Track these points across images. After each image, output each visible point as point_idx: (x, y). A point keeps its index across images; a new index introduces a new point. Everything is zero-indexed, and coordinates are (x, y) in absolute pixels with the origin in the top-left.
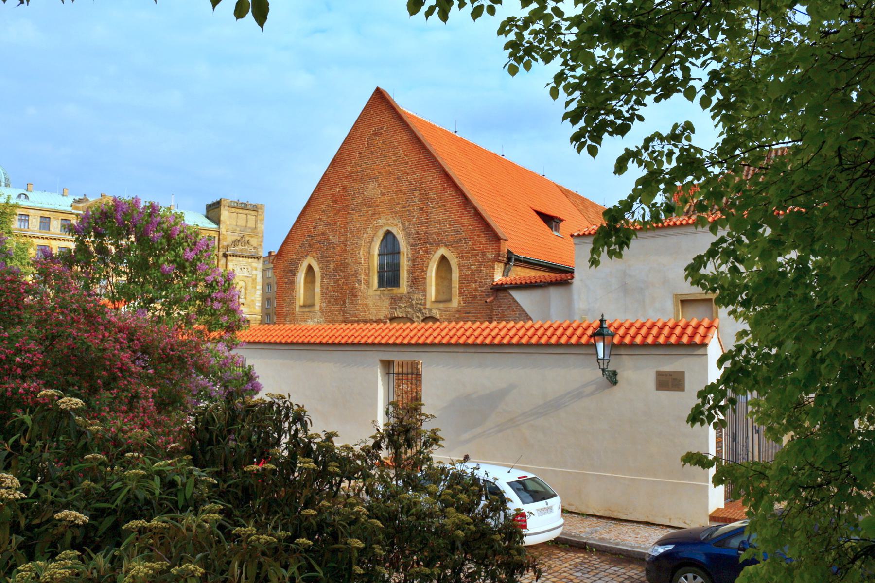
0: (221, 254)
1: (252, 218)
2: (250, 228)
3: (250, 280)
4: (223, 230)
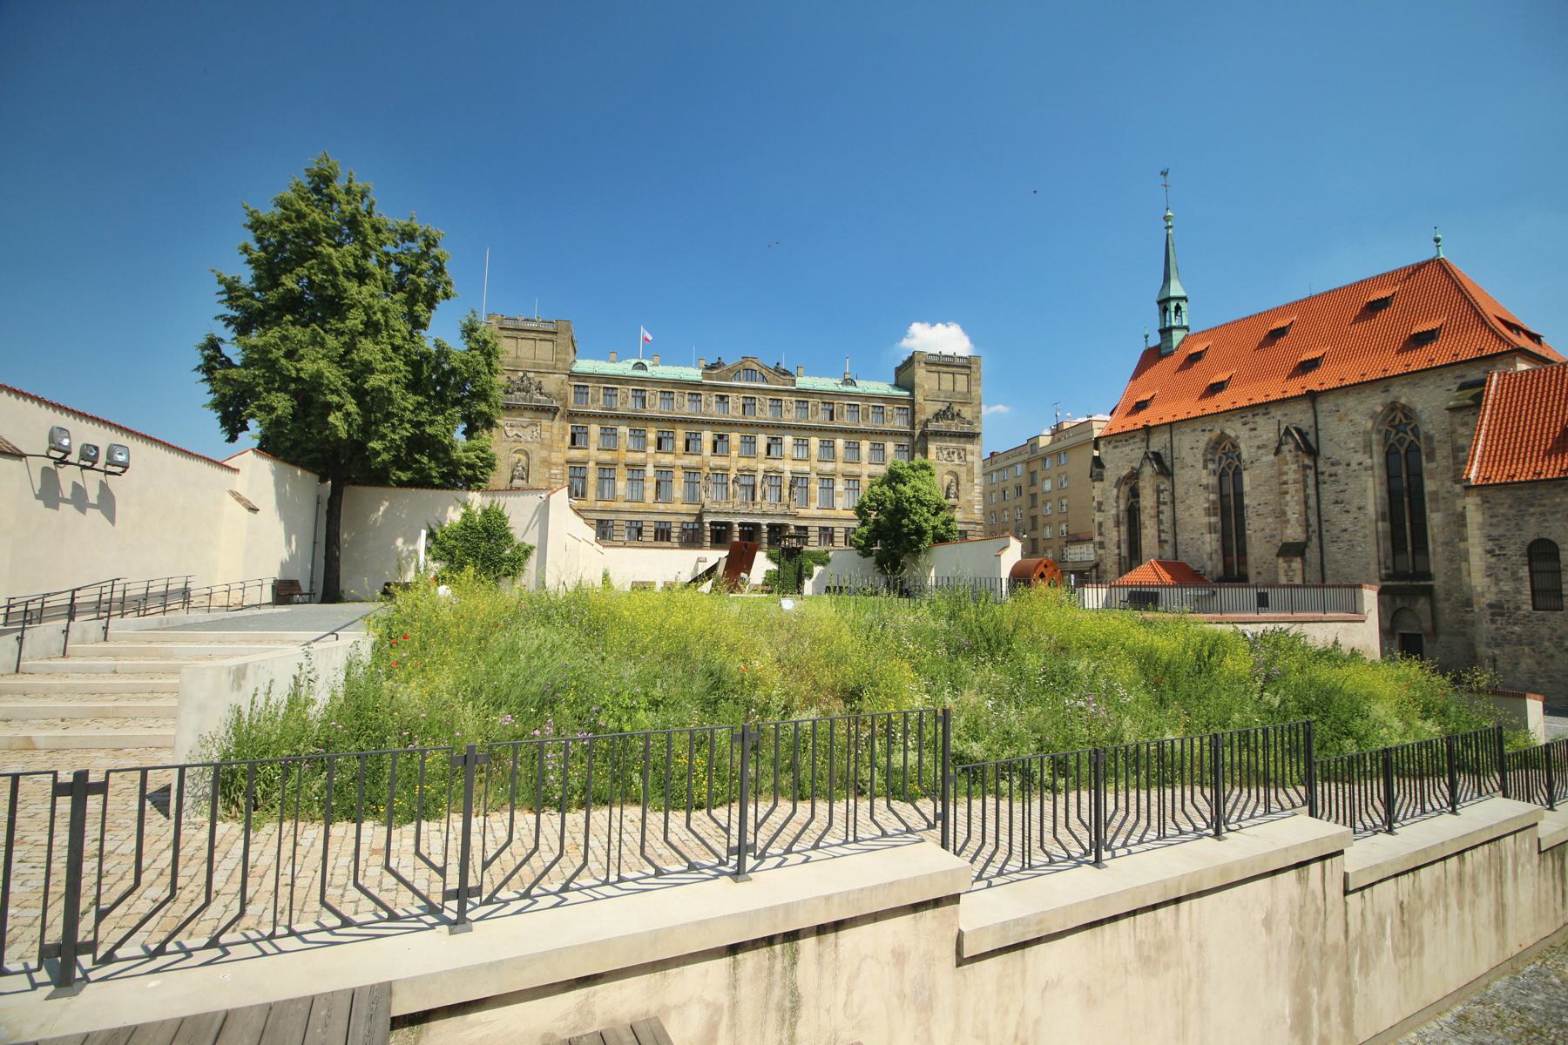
0: (917, 432)
1: (961, 381)
2: (959, 393)
3: (964, 469)
4: (919, 398)
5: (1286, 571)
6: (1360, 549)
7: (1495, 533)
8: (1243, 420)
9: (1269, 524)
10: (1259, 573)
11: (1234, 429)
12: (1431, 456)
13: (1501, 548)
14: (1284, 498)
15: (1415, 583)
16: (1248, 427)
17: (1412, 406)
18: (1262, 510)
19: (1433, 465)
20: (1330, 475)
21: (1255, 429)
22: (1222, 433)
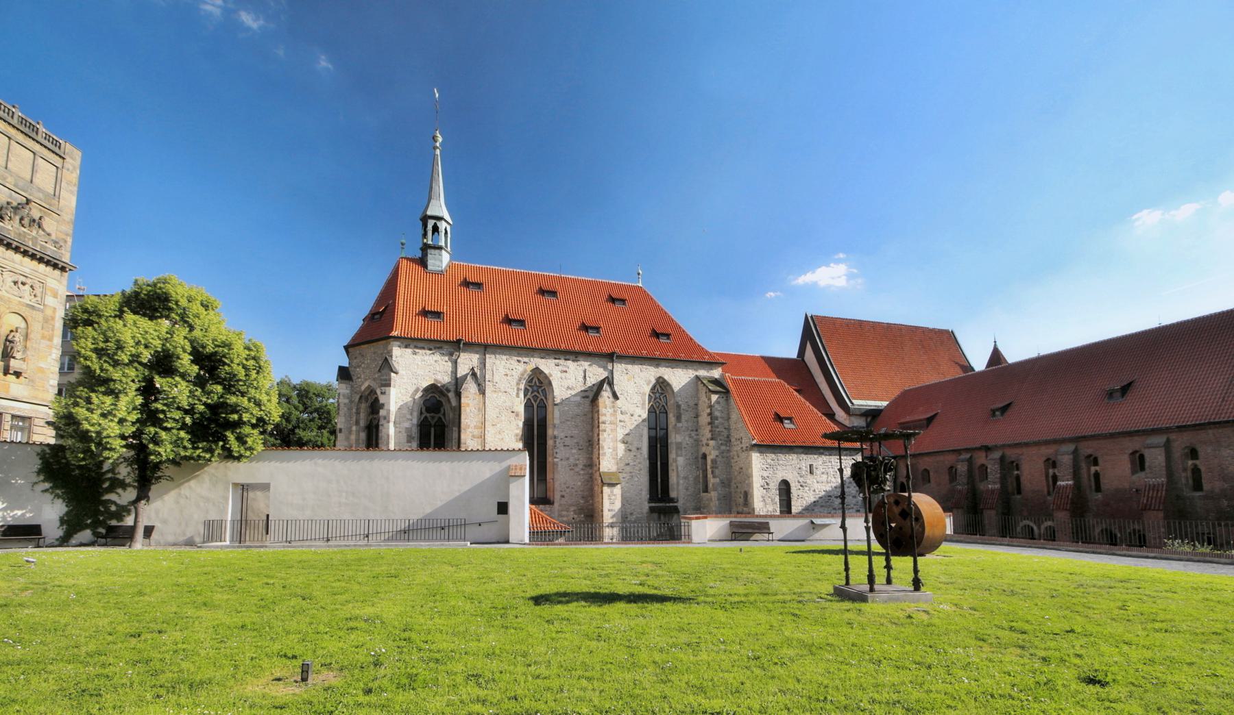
5: (609, 496)
6: (636, 479)
7: (765, 474)
8: (557, 361)
9: (573, 455)
10: (563, 496)
11: (548, 366)
12: (679, 418)
13: (767, 484)
14: (603, 435)
15: (668, 505)
16: (560, 368)
17: (670, 382)
18: (568, 441)
19: (679, 425)
20: (620, 421)
21: (566, 372)
22: (537, 368)
